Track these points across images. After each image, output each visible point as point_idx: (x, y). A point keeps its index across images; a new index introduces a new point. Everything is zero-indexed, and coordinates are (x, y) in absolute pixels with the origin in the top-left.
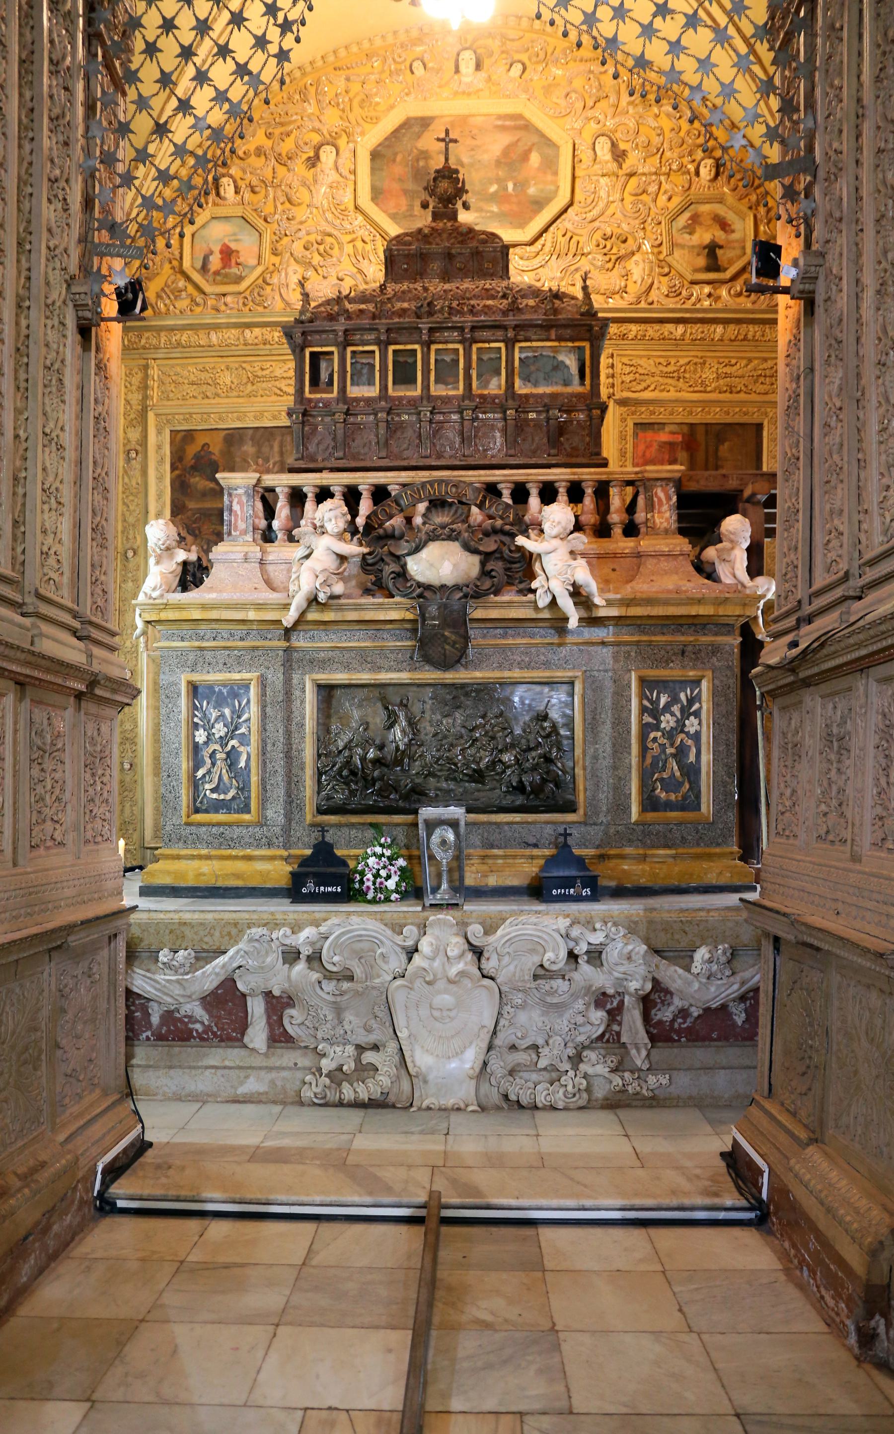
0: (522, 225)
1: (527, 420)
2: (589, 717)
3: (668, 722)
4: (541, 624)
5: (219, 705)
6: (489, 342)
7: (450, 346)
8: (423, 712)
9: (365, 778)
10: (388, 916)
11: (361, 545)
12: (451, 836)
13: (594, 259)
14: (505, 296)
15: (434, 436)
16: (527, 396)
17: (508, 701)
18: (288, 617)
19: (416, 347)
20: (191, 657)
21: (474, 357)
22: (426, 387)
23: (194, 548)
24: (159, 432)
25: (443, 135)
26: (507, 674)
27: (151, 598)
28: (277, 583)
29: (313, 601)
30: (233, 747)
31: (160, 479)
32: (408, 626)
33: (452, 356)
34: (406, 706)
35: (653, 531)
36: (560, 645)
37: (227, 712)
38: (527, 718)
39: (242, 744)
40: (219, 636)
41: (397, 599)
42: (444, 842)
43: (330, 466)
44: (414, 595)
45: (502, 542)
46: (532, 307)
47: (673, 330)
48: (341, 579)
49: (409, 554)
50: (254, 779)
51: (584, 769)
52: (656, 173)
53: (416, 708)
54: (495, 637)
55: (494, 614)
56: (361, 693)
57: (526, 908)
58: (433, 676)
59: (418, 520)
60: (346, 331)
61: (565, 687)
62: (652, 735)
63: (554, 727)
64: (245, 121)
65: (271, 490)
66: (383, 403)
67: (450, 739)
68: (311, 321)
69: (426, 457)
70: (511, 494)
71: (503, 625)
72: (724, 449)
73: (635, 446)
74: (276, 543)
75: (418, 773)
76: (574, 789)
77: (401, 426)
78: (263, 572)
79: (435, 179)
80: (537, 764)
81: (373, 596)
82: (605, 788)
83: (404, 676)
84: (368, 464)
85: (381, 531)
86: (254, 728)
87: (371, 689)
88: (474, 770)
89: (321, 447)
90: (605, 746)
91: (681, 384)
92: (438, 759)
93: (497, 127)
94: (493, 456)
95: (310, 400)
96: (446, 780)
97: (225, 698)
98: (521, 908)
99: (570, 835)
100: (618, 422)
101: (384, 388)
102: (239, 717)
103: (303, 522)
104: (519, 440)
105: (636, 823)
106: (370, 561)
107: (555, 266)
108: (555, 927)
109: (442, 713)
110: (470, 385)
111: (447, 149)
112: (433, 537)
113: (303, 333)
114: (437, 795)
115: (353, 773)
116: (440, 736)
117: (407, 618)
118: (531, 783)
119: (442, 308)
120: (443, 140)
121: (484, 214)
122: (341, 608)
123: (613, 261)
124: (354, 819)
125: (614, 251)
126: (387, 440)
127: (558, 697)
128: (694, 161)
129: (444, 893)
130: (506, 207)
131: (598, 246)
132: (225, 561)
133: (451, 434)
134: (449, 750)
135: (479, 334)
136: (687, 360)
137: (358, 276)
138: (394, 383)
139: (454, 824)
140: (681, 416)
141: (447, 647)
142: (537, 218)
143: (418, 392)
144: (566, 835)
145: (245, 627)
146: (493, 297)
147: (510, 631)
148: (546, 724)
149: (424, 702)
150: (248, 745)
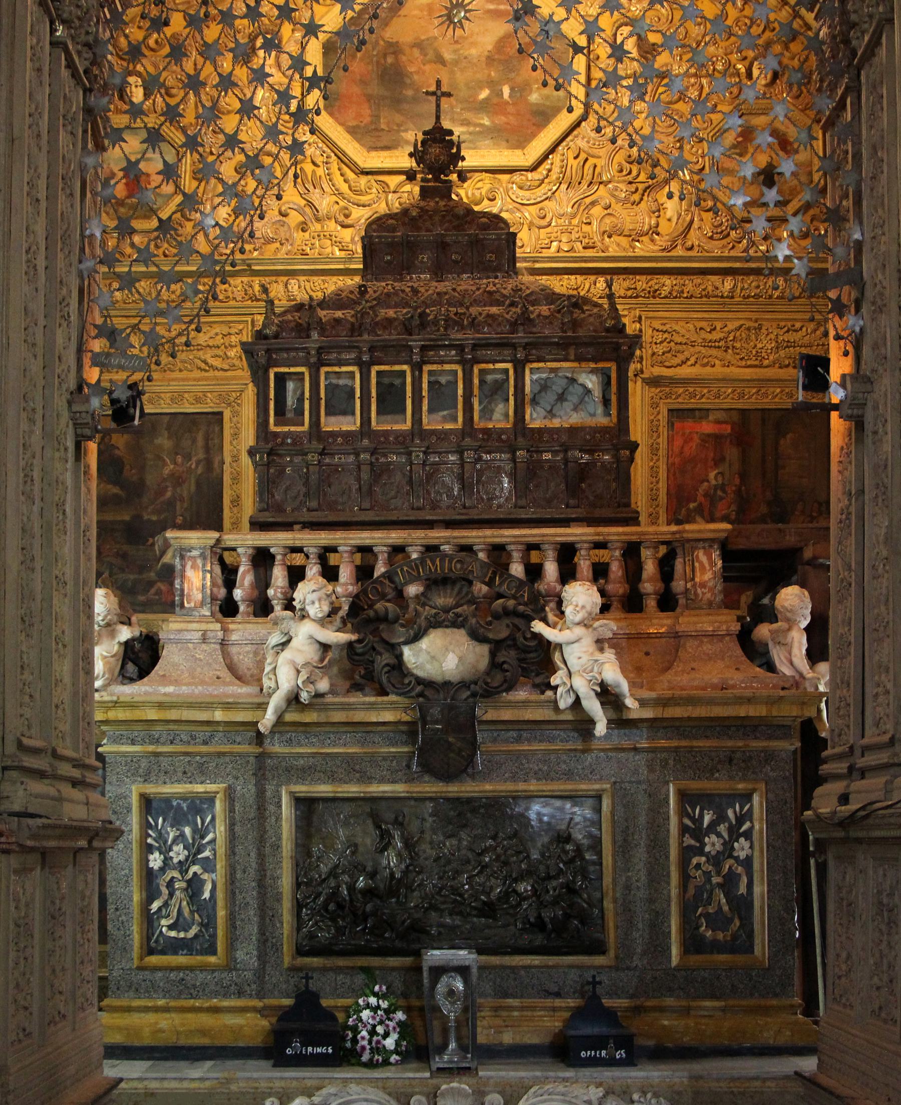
0: (521, 144)
2: (619, 838)
3: (713, 845)
5: (177, 823)
8: (422, 832)
9: (355, 915)
10: (391, 1083)
12: (460, 985)
13: (616, 189)
15: (428, 482)
16: (540, 431)
17: (523, 819)
20: (144, 764)
26: (521, 786)
29: (294, 700)
30: (195, 874)
33: (450, 378)
34: (401, 824)
37: (187, 831)
38: (546, 839)
39: (206, 870)
41: (392, 698)
42: (451, 993)
44: (413, 694)
45: (515, 626)
47: (718, 284)
49: (407, 642)
50: (221, 913)
51: (615, 901)
53: (414, 826)
56: (347, 808)
57: (551, 1074)
58: (434, 789)
61: (590, 802)
62: (695, 861)
63: (579, 850)
64: (256, 218)
67: (454, 865)
68: (276, 336)
69: (419, 509)
71: (516, 727)
72: (786, 443)
73: (670, 440)
74: (239, 618)
75: (416, 906)
76: (603, 927)
77: (387, 469)
78: (226, 655)
79: (424, 143)
80: (559, 895)
82: (640, 926)
83: (399, 789)
85: (371, 613)
86: (221, 850)
87: (360, 803)
88: (484, 902)
90: (640, 874)
91: (729, 355)
92: (441, 889)
93: (489, 11)
94: (499, 506)
95: (276, 435)
96: (451, 915)
97: (185, 815)
98: (545, 1074)
99: (600, 983)
100: (647, 408)
102: (203, 837)
105: (678, 969)
106: (360, 651)
107: (565, 199)
108: (586, 1098)
109: (444, 834)
112: (435, 624)
113: (268, 351)
114: (440, 933)
115: (340, 906)
116: (443, 861)
118: (552, 919)
121: (471, 129)
122: (325, 708)
123: (640, 191)
124: (341, 962)
125: (642, 177)
126: (371, 486)
127: (581, 813)
128: (745, 58)
129: (450, 1055)
130: (501, 120)
131: (621, 171)
132: (178, 642)
134: (454, 879)
136: (737, 324)
139: (463, 971)
140: (730, 400)
142: (542, 135)
143: (407, 426)
144: (595, 983)
148: (569, 847)
149: (424, 820)
150: (213, 871)
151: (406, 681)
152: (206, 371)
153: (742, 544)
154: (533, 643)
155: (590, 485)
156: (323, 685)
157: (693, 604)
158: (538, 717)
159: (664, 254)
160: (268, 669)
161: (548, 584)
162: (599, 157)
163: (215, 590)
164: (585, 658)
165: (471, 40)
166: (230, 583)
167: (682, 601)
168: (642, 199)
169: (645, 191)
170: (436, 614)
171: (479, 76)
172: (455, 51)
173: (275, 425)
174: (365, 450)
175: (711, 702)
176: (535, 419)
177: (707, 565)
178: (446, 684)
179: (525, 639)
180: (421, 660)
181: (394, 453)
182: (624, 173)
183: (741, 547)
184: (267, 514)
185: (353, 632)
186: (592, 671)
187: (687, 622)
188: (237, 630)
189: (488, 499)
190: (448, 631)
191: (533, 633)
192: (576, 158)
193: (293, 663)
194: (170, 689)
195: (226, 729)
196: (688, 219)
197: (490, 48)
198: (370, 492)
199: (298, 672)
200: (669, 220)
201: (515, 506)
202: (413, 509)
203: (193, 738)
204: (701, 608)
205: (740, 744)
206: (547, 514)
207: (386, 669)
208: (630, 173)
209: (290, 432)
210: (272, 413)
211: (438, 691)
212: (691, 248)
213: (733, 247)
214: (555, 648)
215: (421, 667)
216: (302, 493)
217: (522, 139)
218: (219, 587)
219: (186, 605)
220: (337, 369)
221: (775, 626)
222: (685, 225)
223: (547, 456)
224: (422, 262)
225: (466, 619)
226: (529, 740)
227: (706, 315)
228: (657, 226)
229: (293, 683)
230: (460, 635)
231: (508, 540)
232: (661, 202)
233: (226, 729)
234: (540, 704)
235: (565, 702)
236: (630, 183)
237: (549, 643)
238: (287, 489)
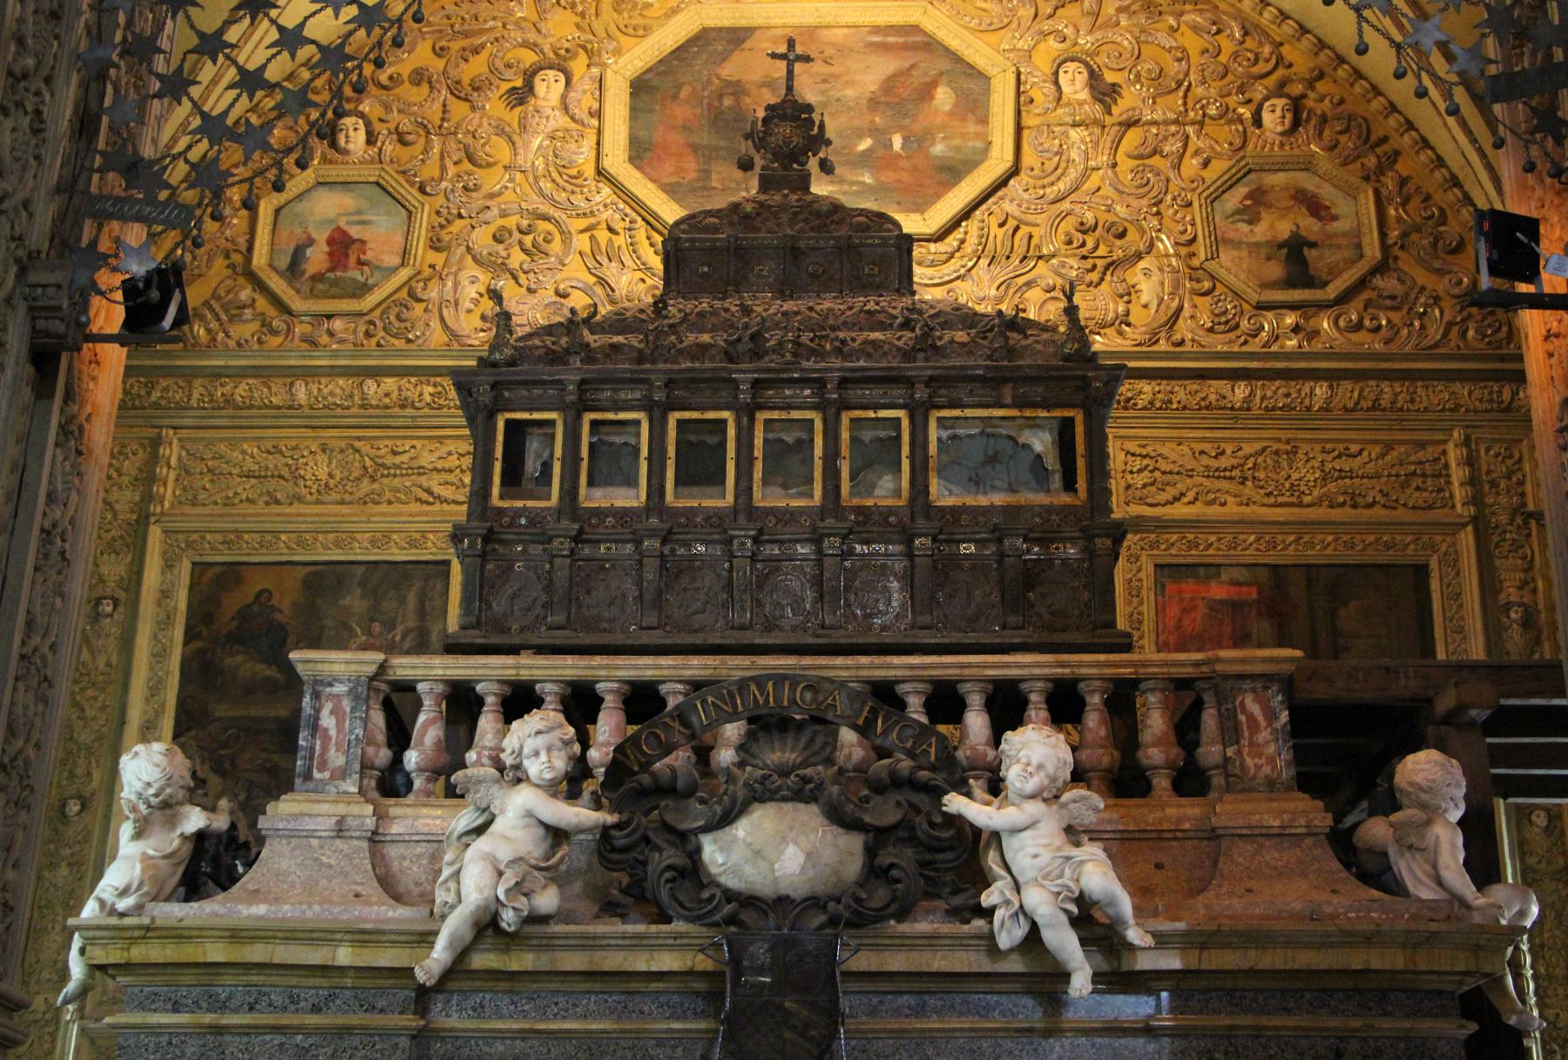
0: (920, 208)
1: (955, 558)
4: (1003, 987)
6: (876, 407)
7: (796, 415)
11: (598, 806)
14: (907, 325)
15: (760, 587)
18: (428, 962)
19: (725, 414)
21: (845, 436)
22: (744, 489)
23: (224, 803)
24: (169, 564)
25: (782, 49)
27: (113, 912)
28: (406, 883)
29: (487, 926)
31: (159, 655)
32: (699, 986)
35: (1238, 782)
36: (1048, 1033)
40: (264, 1001)
41: (678, 926)
43: (536, 641)
44: (718, 917)
45: (911, 805)
46: (963, 345)
48: (553, 880)
49: (707, 829)
52: (1176, 122)
54: (897, 1012)
55: (897, 962)
59: (725, 756)
60: (583, 382)
65: (408, 687)
66: (654, 521)
68: (512, 363)
69: (742, 628)
70: (926, 705)
71: (916, 986)
74: (411, 799)
77: (691, 566)
79: (765, 121)
81: (624, 917)
84: (619, 639)
85: (646, 779)
89: (520, 604)
94: (884, 628)
95: (501, 512)
101: (656, 490)
103: (471, 756)
104: (940, 596)
106: (619, 843)
107: (986, 277)
110: (838, 488)
111: (790, 73)
117: (700, 968)
119: (780, 344)
120: (783, 57)
121: (846, 187)
122: (548, 944)
123: (1100, 268)
125: (1102, 251)
126: (659, 594)
130: (888, 177)
131: (1070, 242)
132: (291, 835)
133: (796, 583)
135: (855, 393)
137: (599, 290)
138: (678, 482)
141: (788, 1035)
142: (950, 195)
145: (324, 982)
146: (882, 327)
147: (932, 1001)
151: (705, 895)
152: (428, 503)
153: (1319, 692)
154: (946, 834)
155: (1043, 596)
156: (547, 900)
157: (1238, 782)
158: (958, 967)
159: (1144, 349)
160: (447, 872)
161: (972, 748)
162: (1037, 225)
163: (370, 750)
164: (1046, 857)
165: (847, 78)
166: (400, 737)
167: (1218, 780)
168: (1102, 279)
169: (1107, 268)
170: (764, 778)
171: (857, 122)
172: (823, 92)
173: (502, 497)
174: (652, 533)
175: (1292, 941)
176: (942, 494)
177: (1261, 719)
178: (783, 901)
179: (932, 825)
180: (734, 858)
181: (702, 542)
182: (1075, 244)
183: (1318, 696)
184: (474, 632)
185: (611, 812)
186: (1061, 876)
187: (1228, 811)
188: (406, 817)
189: (867, 616)
190: (788, 806)
191: (946, 814)
192: (1001, 225)
193: (492, 860)
194: (260, 909)
195: (359, 983)
196: (1175, 304)
197: (874, 88)
198: (658, 602)
199: (500, 874)
200: (1145, 306)
201: (913, 627)
202: (732, 628)
203: (294, 1000)
204: (1251, 790)
205: (1356, 1023)
206: (971, 638)
207: (668, 875)
208: (1083, 245)
209: (525, 508)
210: (497, 479)
211: (766, 914)
212: (1182, 343)
213: (1246, 342)
214: (988, 845)
215: (735, 871)
216: (539, 603)
217: (920, 201)
218: (377, 745)
219: (317, 775)
220: (611, 416)
221: (1394, 817)
222: (1170, 313)
223: (968, 549)
224: (759, 276)
225: (820, 786)
226: (939, 1012)
227: (1208, 434)
228: (1127, 313)
229: (488, 893)
230: (809, 815)
231: (899, 673)
232: (1131, 282)
233: (359, 983)
234: (960, 942)
235: (1009, 936)
236: (1084, 258)
237: (977, 832)
238: (514, 596)
